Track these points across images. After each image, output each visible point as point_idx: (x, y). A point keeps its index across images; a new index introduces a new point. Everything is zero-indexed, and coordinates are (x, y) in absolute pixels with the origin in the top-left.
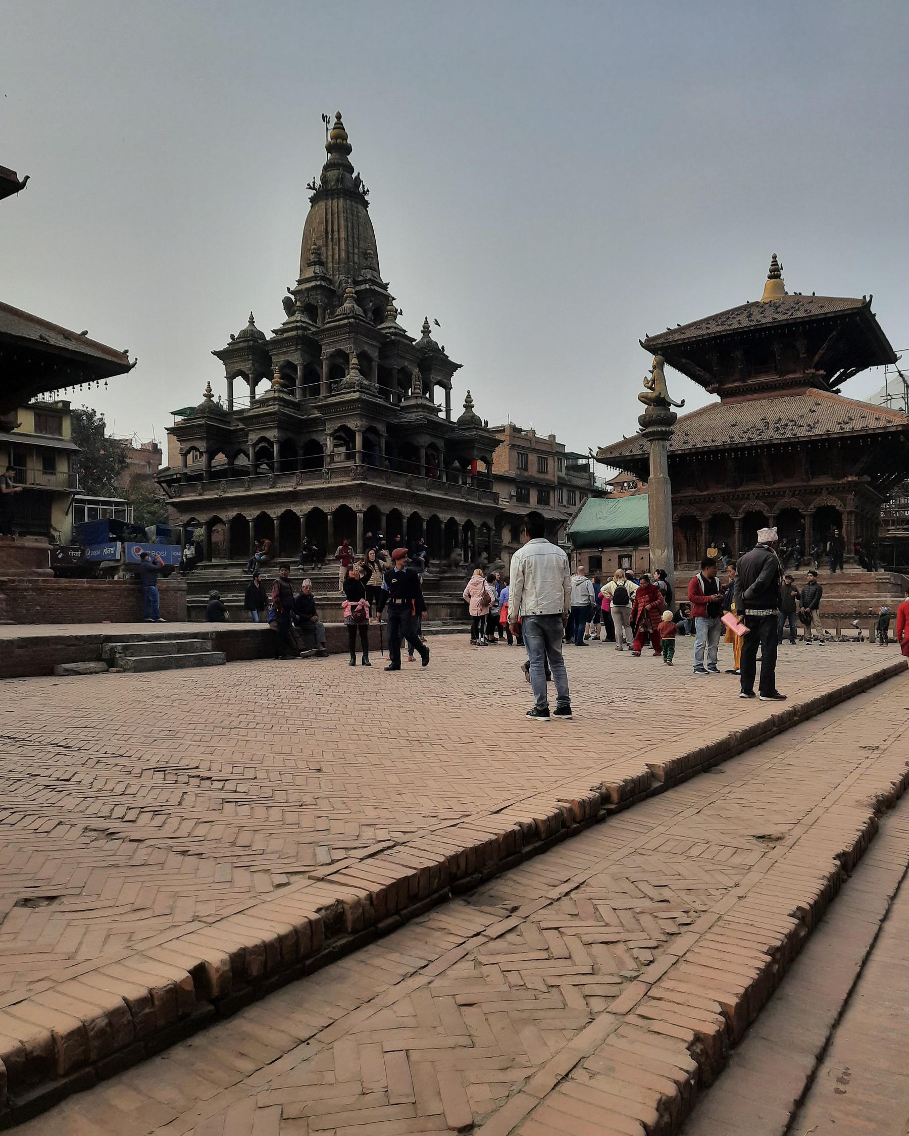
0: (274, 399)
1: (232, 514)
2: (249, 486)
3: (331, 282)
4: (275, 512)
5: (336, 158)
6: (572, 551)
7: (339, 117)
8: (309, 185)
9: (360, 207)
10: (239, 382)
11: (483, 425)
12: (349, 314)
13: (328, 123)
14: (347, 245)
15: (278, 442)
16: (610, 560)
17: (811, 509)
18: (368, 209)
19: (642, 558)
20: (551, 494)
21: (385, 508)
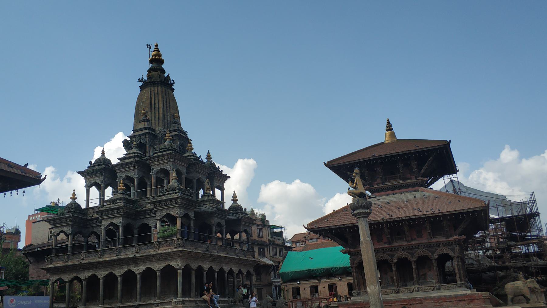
0: (121, 199)
1: (88, 274)
2: (101, 255)
3: (154, 130)
4: (119, 272)
5: (155, 66)
6: (281, 284)
7: (157, 46)
8: (139, 79)
9: (170, 91)
10: (94, 190)
11: (244, 210)
12: (169, 148)
13: (150, 48)
14: (164, 111)
15: (122, 226)
16: (305, 289)
17: (436, 256)
18: (173, 93)
19: (324, 287)
20: (266, 249)
21: (194, 266)
